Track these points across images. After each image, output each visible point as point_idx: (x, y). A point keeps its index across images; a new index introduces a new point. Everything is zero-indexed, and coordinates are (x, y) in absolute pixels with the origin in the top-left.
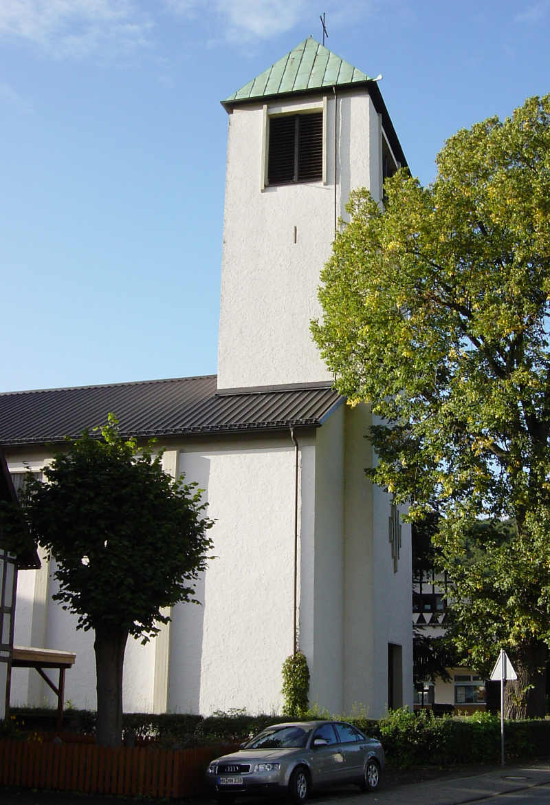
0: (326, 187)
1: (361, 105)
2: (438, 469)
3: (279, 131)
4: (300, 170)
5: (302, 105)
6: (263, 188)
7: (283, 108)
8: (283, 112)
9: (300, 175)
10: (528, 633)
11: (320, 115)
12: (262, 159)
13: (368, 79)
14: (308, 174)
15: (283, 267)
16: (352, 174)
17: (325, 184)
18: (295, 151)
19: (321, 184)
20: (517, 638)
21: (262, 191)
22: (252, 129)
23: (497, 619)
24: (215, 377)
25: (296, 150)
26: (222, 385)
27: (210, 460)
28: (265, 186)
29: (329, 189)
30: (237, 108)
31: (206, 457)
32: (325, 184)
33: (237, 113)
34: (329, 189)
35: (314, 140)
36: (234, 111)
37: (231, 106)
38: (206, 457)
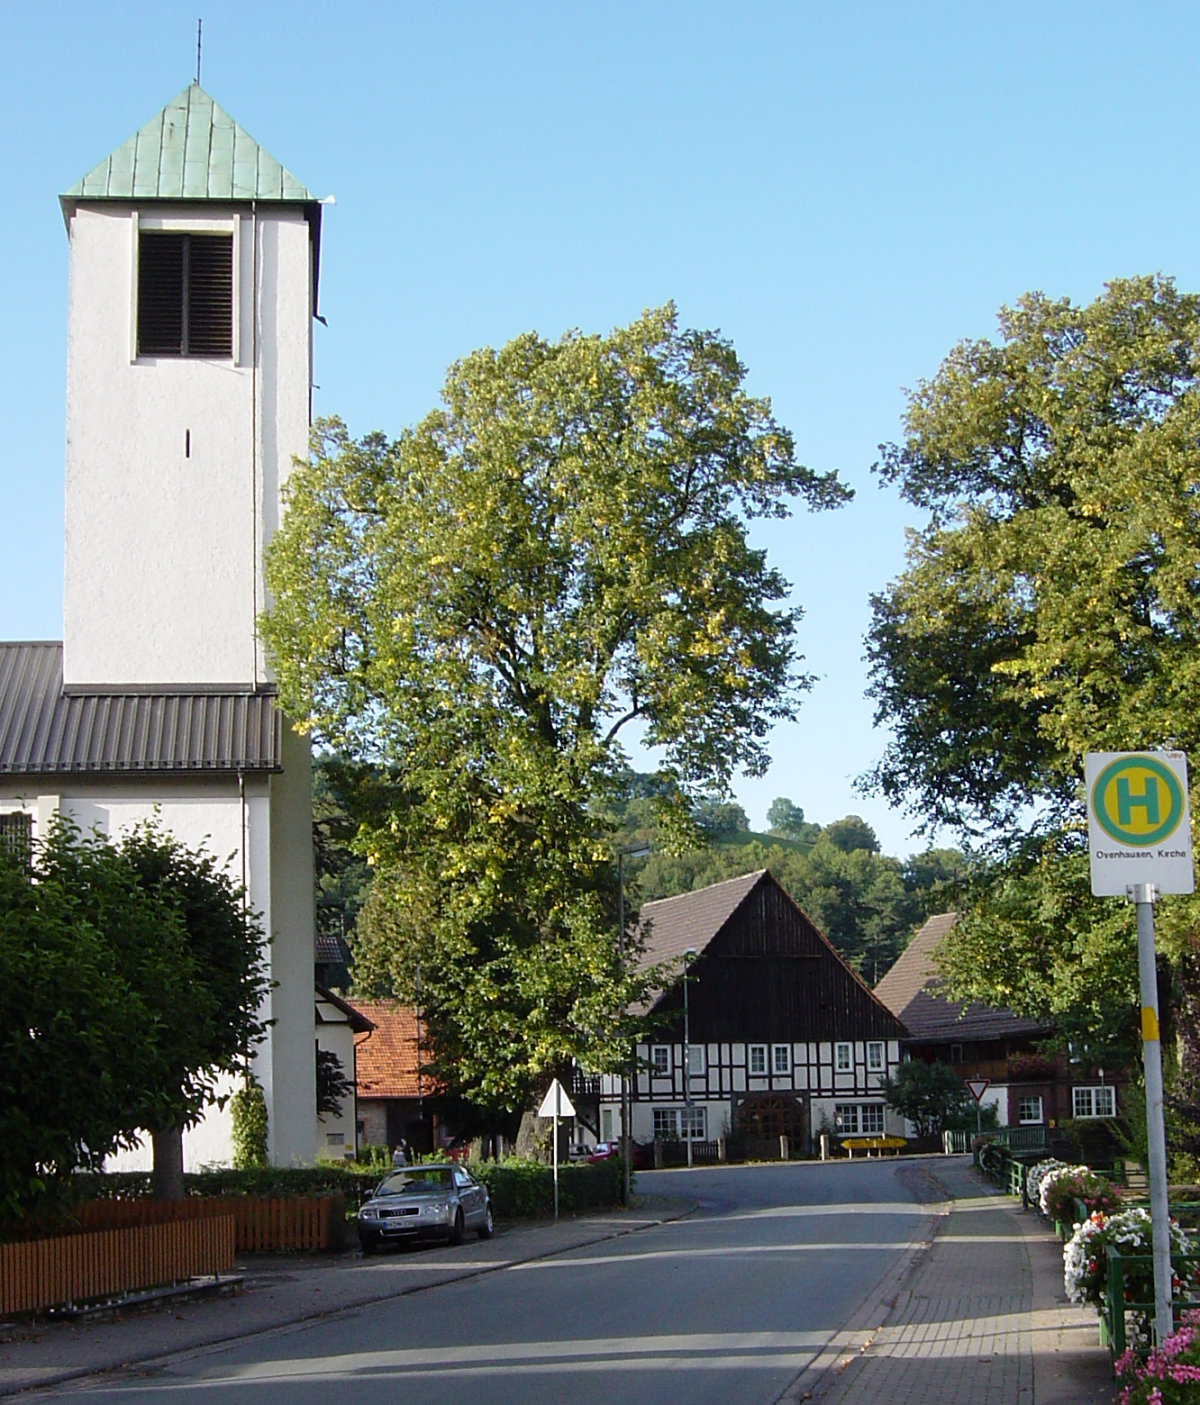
0: (237, 369)
1: (293, 234)
2: (773, 444)
3: (155, 251)
4: (192, 331)
5: (197, 221)
6: (134, 358)
7: (164, 221)
8: (165, 228)
9: (192, 341)
10: (556, 1056)
11: (229, 239)
12: (132, 307)
13: (310, 198)
14: (205, 341)
15: (169, 496)
16: (279, 353)
17: (237, 365)
18: (184, 298)
19: (229, 364)
20: (540, 1062)
21: (133, 363)
22: (111, 251)
23: (518, 1039)
24: (60, 646)
25: (185, 296)
26: (77, 671)
27: (108, 812)
28: (137, 356)
29: (241, 374)
30: (83, 208)
31: (103, 806)
32: (237, 365)
33: (83, 217)
34: (241, 374)
35: (215, 284)
36: (78, 211)
37: (73, 205)
38: (103, 806)
